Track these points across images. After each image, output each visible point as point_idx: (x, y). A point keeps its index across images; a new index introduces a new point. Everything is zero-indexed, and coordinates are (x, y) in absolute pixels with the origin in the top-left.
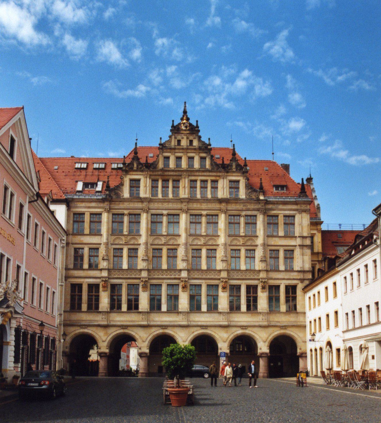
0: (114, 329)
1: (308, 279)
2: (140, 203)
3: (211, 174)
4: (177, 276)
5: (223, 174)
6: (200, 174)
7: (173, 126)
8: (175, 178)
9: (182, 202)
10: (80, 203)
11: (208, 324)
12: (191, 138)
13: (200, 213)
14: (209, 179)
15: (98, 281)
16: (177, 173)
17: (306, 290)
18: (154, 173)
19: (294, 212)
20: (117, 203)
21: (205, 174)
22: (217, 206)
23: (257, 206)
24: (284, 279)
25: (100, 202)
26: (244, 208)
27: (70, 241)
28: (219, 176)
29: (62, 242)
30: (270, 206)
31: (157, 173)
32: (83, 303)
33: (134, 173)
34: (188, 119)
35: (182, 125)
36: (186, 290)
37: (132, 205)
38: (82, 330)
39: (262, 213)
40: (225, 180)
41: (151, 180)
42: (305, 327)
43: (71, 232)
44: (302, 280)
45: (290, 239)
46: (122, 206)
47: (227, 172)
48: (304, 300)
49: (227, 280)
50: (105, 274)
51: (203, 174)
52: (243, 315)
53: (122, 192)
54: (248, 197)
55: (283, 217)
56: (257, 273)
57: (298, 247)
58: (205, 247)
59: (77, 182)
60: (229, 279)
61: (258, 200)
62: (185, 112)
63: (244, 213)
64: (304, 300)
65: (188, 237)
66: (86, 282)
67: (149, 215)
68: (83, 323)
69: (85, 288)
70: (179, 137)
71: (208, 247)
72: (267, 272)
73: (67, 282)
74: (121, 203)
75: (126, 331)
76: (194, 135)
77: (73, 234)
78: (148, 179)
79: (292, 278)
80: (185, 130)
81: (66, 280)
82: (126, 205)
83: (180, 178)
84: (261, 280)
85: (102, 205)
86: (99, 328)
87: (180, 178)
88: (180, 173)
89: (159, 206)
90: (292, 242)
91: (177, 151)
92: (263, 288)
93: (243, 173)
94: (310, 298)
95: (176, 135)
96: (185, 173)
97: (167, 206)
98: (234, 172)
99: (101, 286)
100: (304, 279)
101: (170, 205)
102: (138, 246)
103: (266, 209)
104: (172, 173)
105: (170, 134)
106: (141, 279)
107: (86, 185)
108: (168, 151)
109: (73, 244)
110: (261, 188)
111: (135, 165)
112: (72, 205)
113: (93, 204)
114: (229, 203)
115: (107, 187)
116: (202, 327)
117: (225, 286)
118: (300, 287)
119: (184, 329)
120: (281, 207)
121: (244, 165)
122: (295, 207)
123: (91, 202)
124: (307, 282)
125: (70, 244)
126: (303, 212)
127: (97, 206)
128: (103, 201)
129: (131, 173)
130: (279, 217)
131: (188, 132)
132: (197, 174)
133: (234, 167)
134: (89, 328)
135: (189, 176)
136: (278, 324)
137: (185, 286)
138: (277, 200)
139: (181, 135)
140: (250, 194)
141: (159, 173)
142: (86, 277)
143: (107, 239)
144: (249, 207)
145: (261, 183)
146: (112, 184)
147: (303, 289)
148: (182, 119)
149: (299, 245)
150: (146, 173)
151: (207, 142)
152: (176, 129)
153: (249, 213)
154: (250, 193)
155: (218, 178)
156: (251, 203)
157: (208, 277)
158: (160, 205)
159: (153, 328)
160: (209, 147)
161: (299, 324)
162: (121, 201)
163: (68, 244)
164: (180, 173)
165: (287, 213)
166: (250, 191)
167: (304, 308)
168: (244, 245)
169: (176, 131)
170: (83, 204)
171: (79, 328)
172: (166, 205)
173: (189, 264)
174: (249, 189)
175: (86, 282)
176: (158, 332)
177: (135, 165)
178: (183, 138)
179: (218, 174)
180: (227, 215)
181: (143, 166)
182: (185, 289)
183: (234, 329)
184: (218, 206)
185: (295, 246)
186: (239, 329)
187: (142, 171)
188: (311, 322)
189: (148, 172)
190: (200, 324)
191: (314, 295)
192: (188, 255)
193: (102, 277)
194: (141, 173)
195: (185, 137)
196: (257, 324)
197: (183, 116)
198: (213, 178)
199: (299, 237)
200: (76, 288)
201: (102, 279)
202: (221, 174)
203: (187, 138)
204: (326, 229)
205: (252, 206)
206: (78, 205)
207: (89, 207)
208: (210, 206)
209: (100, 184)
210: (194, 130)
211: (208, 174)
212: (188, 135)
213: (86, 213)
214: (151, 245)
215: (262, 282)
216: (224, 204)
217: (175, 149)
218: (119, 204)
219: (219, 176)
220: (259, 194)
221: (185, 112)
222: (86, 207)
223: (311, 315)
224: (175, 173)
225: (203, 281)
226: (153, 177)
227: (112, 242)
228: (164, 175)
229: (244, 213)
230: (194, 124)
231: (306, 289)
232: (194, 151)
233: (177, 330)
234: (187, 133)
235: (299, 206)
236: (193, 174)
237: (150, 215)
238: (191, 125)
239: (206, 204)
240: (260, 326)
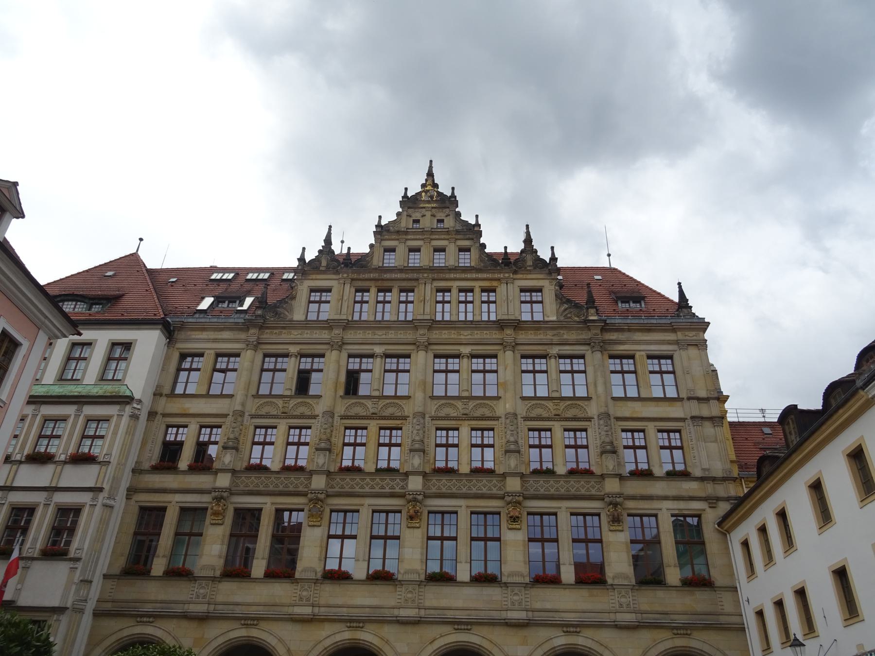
0: (223, 626)
1: (727, 499)
2: (326, 332)
3: (480, 276)
4: (397, 490)
5: (507, 275)
6: (458, 276)
7: (405, 196)
8: (404, 284)
9: (416, 328)
10: (197, 333)
11: (474, 615)
12: (440, 215)
13: (457, 352)
14: (477, 285)
15: (206, 498)
16: (410, 276)
17: (727, 525)
18: (362, 276)
19: (671, 347)
20: (275, 331)
21: (469, 276)
22: (495, 335)
23: (585, 336)
24: (666, 498)
25: (240, 330)
26: (556, 339)
27: (160, 410)
28: (499, 280)
29: (135, 405)
30: (614, 336)
31: (367, 276)
32: (158, 557)
33: (319, 277)
34: (436, 186)
35: (423, 194)
36: (418, 525)
37: (307, 335)
38: (139, 630)
39: (597, 348)
40: (510, 286)
41: (353, 290)
42: (742, 629)
43: (167, 390)
44: (713, 501)
45: (667, 403)
46: (285, 336)
47: (515, 272)
48: (727, 555)
49: (521, 498)
50: (223, 481)
51: (463, 276)
52: (567, 592)
53: (291, 310)
54: (562, 318)
55: (645, 357)
56: (595, 482)
57: (689, 422)
58: (467, 423)
59: (203, 298)
60: (526, 498)
61: (586, 321)
62: (430, 174)
63: (555, 350)
64: (726, 551)
65: (429, 400)
66: (174, 503)
67: (344, 355)
68: (148, 608)
69: (171, 519)
70: (417, 215)
71: (474, 423)
72: (620, 479)
73: (132, 502)
74: (284, 331)
75: (254, 633)
76: (447, 210)
77: (172, 395)
78: (347, 287)
79: (684, 494)
80: (428, 202)
81: (128, 498)
82: (295, 335)
83: (415, 284)
84: (607, 499)
85: (243, 336)
86: (185, 624)
87: (415, 284)
88: (415, 276)
89: (367, 336)
90: (676, 411)
91: (409, 237)
92: (616, 520)
93: (550, 273)
94: (745, 544)
95: (410, 211)
96: (426, 275)
97: (384, 336)
98: (530, 272)
99: (209, 512)
100: (718, 499)
101: (391, 335)
102: (313, 421)
103: (604, 342)
104: (399, 276)
105: (401, 210)
106: (309, 496)
107: (218, 300)
108: (393, 237)
109: (165, 415)
110: (591, 302)
111: (324, 263)
112: (181, 335)
113: (226, 335)
114: (522, 329)
115: (261, 303)
116: (458, 624)
117: (517, 514)
118: (711, 517)
119: (409, 629)
120: (639, 336)
121: (551, 259)
122: (671, 337)
123: (221, 330)
124: (724, 507)
125: (159, 417)
126: (690, 347)
127: (232, 337)
128: (246, 326)
129: (314, 277)
130: (637, 356)
131: (434, 205)
132: (452, 276)
133: (530, 263)
134: (159, 623)
135: (434, 280)
136: (664, 620)
137: (416, 512)
138: (629, 321)
139: (420, 210)
140: (567, 312)
141: (372, 276)
142: (179, 490)
143: (243, 405)
144: (565, 337)
145: (590, 293)
146: (271, 300)
147: (719, 524)
148: (423, 186)
149: (693, 418)
150: (345, 275)
151: (473, 222)
152: (408, 202)
153: (567, 350)
154: (565, 310)
155: (495, 284)
156: (569, 329)
157: (474, 490)
158: (369, 335)
159: (327, 626)
160: (476, 229)
161: (723, 619)
162: (284, 328)
163: (152, 415)
164: (415, 276)
165: (654, 348)
166: (566, 306)
167: (732, 575)
168: (558, 418)
169: (411, 205)
170: (204, 335)
171: (131, 622)
172: (380, 335)
173: (429, 461)
174: (562, 303)
175: (174, 503)
176: (338, 638)
177: (324, 263)
178: (423, 216)
179: (496, 276)
180: (519, 356)
181: (339, 265)
182: (415, 523)
183: (543, 633)
184: (497, 336)
185: (683, 420)
186: (558, 632)
187: (337, 273)
188: (760, 614)
189: (348, 273)
190: (450, 614)
191: (763, 530)
192: (426, 440)
193: (215, 489)
194: (334, 277)
195: (428, 214)
196: (605, 618)
197: (426, 180)
198: (486, 284)
199: (689, 399)
200: (150, 518)
201: (213, 494)
202: (502, 276)
203: (433, 216)
204: (736, 420)
205: (572, 336)
206: (193, 337)
207: (215, 340)
208: (478, 335)
209: (249, 301)
210: (449, 202)
211: (474, 276)
212: (433, 210)
213: (207, 352)
214: (343, 417)
215: (610, 503)
216: (509, 331)
217: (406, 233)
218: (280, 334)
219: (499, 280)
220: (587, 311)
221: (430, 174)
222: (208, 340)
223: (759, 591)
224: (404, 276)
225: (462, 502)
226: (360, 284)
227: (253, 412)
228: (383, 280)
229: (555, 350)
230: (448, 193)
231: (726, 524)
232: (446, 237)
233: (388, 631)
234: (433, 208)
235: (679, 333)
236: (442, 276)
237: (346, 355)
238: (440, 194)
239: (469, 332)
240: (617, 626)
